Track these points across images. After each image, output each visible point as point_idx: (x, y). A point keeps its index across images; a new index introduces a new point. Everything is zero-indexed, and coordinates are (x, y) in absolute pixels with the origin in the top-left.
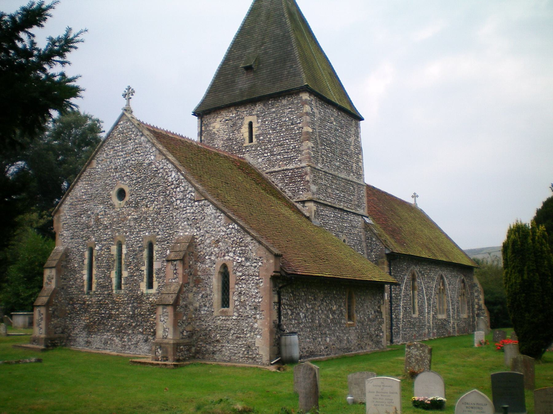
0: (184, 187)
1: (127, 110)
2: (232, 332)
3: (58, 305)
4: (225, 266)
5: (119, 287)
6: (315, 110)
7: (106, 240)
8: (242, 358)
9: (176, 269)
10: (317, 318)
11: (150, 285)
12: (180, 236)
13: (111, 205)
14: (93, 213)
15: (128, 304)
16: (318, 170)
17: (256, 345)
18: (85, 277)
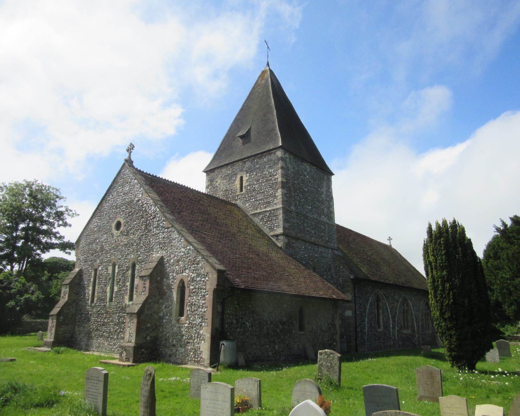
0: (159, 217)
1: (129, 162)
2: (184, 337)
3: (70, 315)
4: (182, 282)
5: (111, 300)
6: (290, 166)
8: (190, 361)
9: (145, 284)
10: (265, 328)
11: (131, 299)
12: (153, 257)
15: (116, 313)
16: (290, 211)
17: (201, 350)
18: (90, 292)
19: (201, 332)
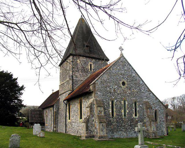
5: (125, 115)
7: (119, 99)
13: (120, 86)
14: (112, 88)
18: (111, 111)
19: (163, 126)
